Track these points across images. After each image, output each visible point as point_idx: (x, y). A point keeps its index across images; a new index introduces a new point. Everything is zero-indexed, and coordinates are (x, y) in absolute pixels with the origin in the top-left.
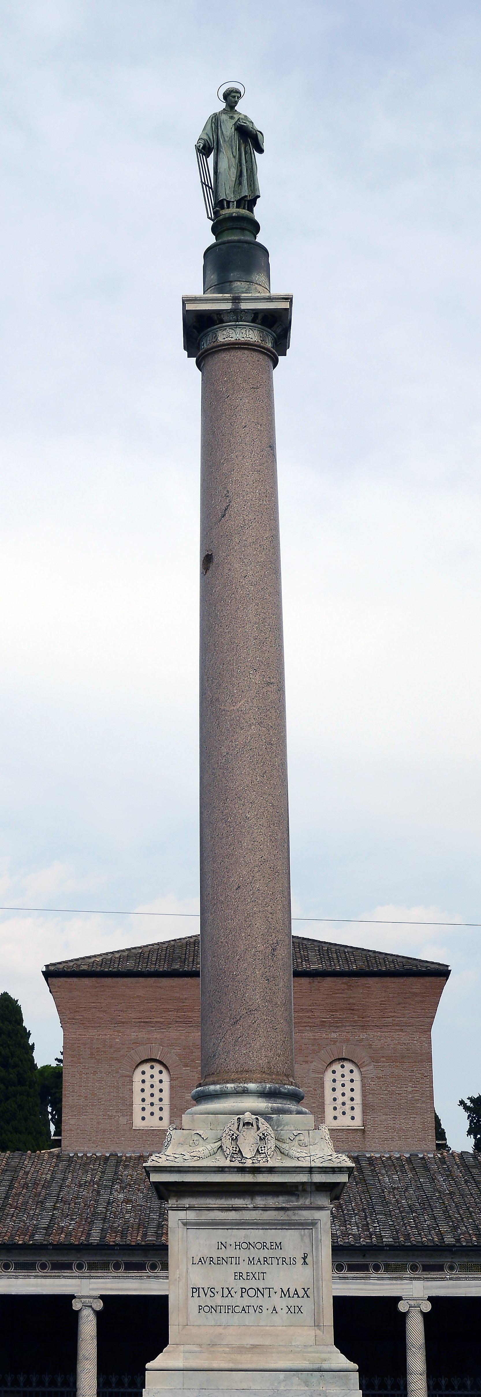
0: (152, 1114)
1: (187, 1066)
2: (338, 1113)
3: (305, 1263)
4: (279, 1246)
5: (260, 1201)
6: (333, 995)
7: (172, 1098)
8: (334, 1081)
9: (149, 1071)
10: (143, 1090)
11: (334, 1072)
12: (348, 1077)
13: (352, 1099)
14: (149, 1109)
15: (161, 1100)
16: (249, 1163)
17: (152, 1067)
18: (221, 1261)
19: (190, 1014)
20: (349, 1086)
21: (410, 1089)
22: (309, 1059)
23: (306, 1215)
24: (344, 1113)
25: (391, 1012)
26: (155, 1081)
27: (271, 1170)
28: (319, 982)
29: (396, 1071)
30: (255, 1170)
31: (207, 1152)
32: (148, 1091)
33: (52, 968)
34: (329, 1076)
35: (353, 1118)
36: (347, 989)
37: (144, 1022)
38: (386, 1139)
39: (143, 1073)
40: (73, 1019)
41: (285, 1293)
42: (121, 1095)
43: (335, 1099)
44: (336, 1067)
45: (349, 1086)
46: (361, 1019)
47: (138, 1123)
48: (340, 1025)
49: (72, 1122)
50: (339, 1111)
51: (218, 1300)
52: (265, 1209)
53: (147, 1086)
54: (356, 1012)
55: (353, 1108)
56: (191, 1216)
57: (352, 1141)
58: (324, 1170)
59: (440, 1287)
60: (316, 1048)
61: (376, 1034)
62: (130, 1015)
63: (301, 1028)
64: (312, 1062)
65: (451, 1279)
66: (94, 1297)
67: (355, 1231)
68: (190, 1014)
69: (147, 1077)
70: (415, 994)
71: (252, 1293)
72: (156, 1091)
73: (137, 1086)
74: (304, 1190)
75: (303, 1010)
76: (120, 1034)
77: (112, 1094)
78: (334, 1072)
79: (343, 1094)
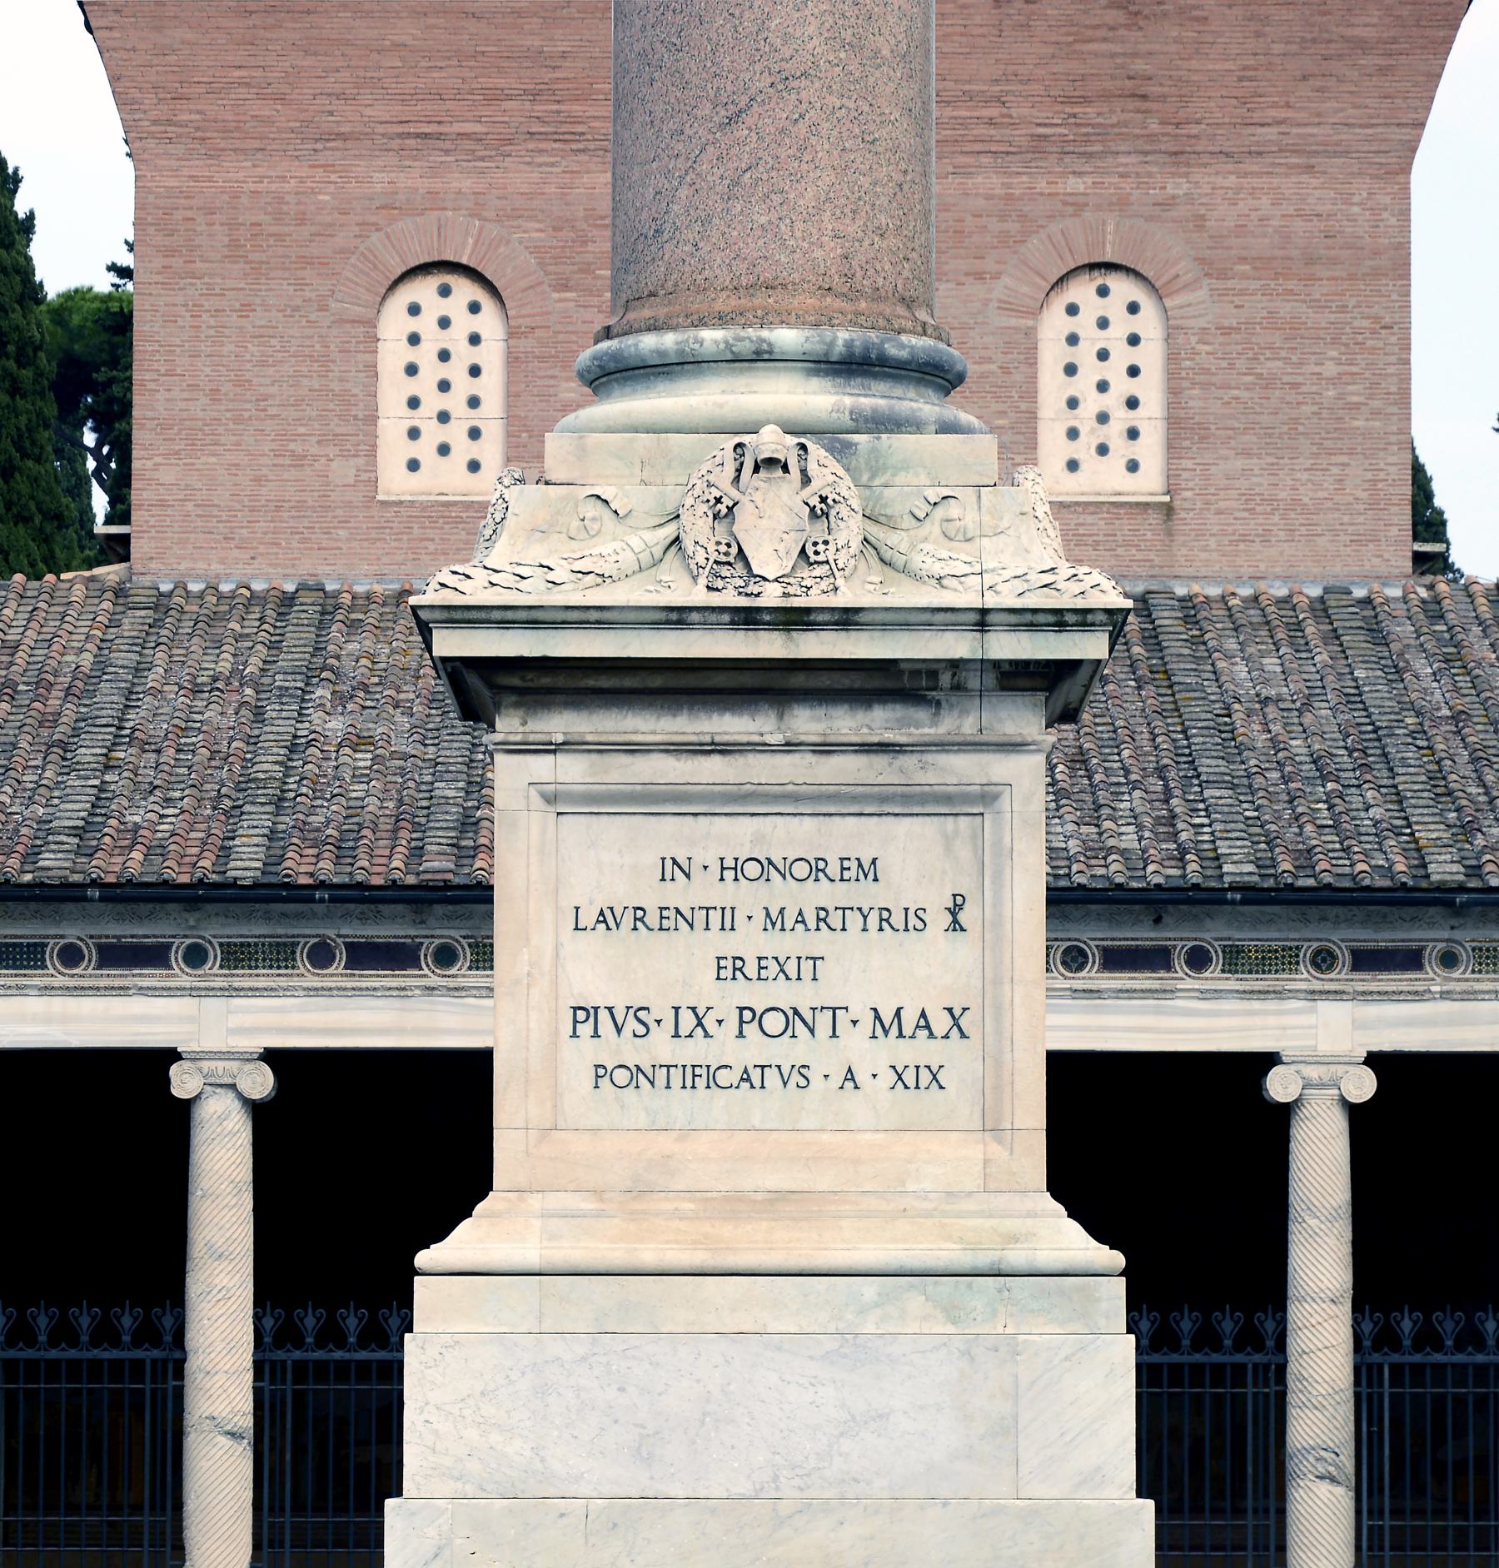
0: (444, 450)
1: (566, 287)
2: (1083, 449)
3: (956, 926)
4: (869, 870)
5: (807, 722)
6: (1078, 47)
7: (512, 396)
8: (1073, 340)
9: (434, 306)
10: (412, 370)
12: (1122, 325)
13: (1132, 403)
14: (433, 433)
15: (474, 402)
16: (771, 596)
17: (445, 291)
18: (672, 919)
19: (576, 108)
20: (1122, 356)
21: (1330, 369)
22: (989, 265)
23: (962, 769)
24: (1103, 450)
25: (1274, 105)
27: (847, 619)
29: (1285, 309)
30: (794, 619)
31: (628, 560)
34: (1053, 324)
35: (1133, 466)
36: (1128, 27)
37: (418, 136)
38: (1244, 538)
39: (414, 310)
40: (170, 123)
41: (885, 1025)
42: (336, 386)
43: (1073, 403)
44: (1082, 291)
46: (1170, 129)
47: (395, 482)
48: (1097, 148)
49: (167, 475)
51: (661, 1047)
52: (824, 748)
53: (426, 356)
54: (1154, 106)
55: (1133, 434)
56: (572, 770)
57: (1127, 544)
58: (1028, 620)
60: (1013, 227)
61: (1219, 181)
62: (368, 111)
63: (962, 160)
64: (997, 276)
67: (1129, 840)
68: (576, 108)
69: (426, 325)
70: (1361, 45)
71: (774, 1022)
72: (455, 370)
73: (392, 354)
74: (958, 687)
75: (970, 96)
76: (333, 177)
77: (305, 381)
78: (1072, 310)
79: (1103, 387)
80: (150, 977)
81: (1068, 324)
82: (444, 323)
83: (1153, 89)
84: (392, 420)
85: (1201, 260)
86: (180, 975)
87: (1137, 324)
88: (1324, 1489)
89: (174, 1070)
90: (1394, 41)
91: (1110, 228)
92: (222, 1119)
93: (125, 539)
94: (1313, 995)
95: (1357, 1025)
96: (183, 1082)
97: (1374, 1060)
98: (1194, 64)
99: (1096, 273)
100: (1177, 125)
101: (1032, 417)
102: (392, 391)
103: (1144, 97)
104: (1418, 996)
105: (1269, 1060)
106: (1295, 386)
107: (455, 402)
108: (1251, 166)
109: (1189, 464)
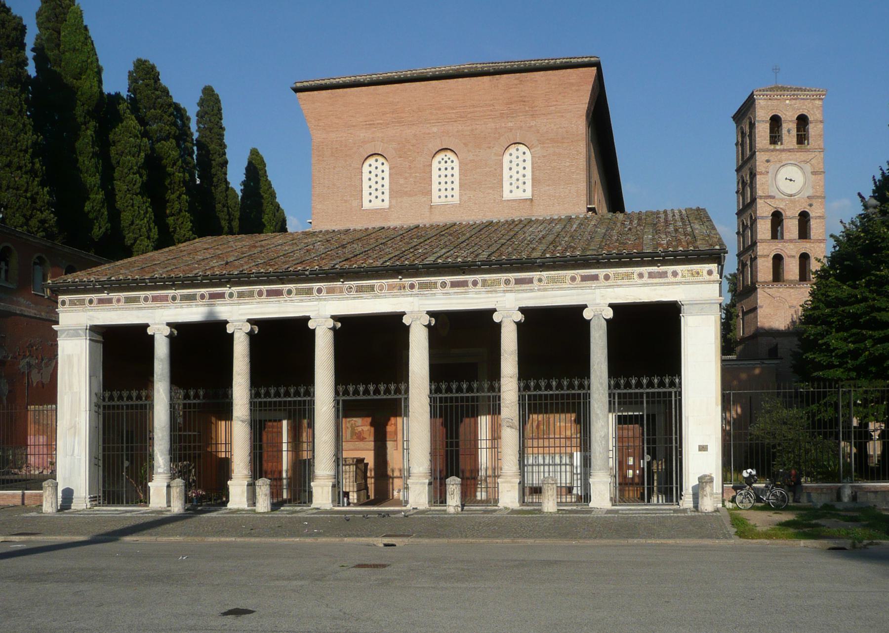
0: (377, 197)
1: (401, 157)
8: (511, 162)
9: (374, 164)
11: (511, 155)
13: (524, 176)
21: (568, 164)
24: (518, 187)
26: (379, 171)
28: (497, 80)
32: (374, 179)
34: (506, 158)
35: (524, 191)
36: (520, 84)
40: (318, 126)
42: (353, 184)
43: (511, 177)
44: (512, 149)
45: (522, 165)
47: (366, 205)
48: (515, 115)
50: (514, 185)
53: (373, 176)
54: (527, 103)
59: (530, 298)
60: (497, 135)
65: (539, 290)
69: (373, 169)
73: (366, 176)
77: (347, 183)
78: (511, 155)
84: (366, 191)
85: (538, 140)
87: (525, 157)
91: (518, 134)
95: (517, 300)
99: (516, 145)
100: (532, 108)
102: (366, 184)
103: (524, 101)
104: (532, 290)
105: (494, 310)
106: (559, 169)
107: (379, 186)
108: (550, 117)
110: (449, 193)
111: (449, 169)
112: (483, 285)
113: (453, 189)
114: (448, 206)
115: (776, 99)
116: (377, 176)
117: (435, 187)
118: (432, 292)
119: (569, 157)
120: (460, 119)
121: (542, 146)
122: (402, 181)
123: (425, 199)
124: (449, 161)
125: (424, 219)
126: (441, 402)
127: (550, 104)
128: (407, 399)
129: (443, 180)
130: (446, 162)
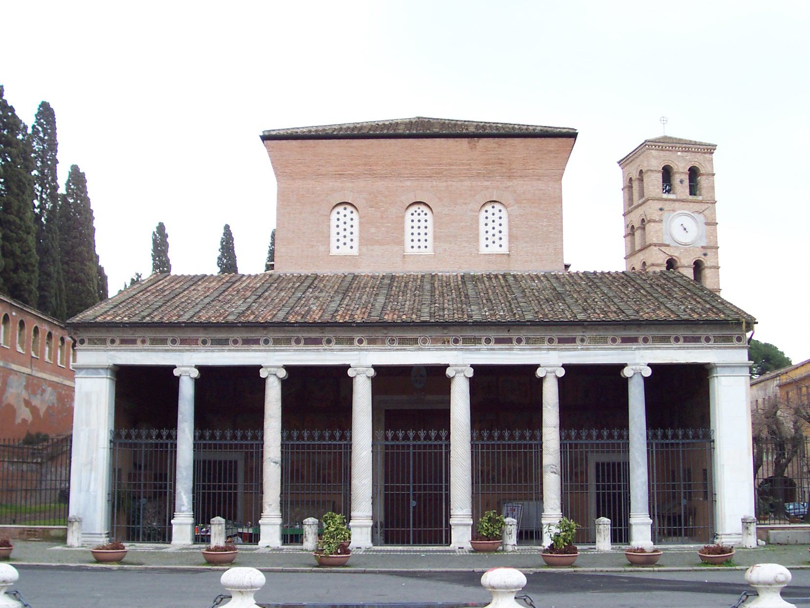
0: (345, 244)
7: (360, 231)
8: (487, 218)
12: (498, 215)
13: (500, 232)
14: (342, 240)
17: (345, 209)
19: (374, 168)
20: (498, 221)
21: (545, 224)
25: (531, 165)
26: (348, 219)
32: (342, 226)
33: (266, 134)
37: (339, 174)
38: (526, 261)
39: (338, 213)
44: (489, 207)
47: (334, 251)
48: (491, 175)
50: (491, 239)
53: (341, 223)
54: (504, 165)
55: (501, 239)
64: (469, 203)
66: (278, 367)
69: (341, 216)
70: (550, 151)
72: (348, 226)
73: (334, 222)
75: (463, 164)
78: (486, 211)
80: (255, 347)
81: (485, 214)
82: (345, 216)
83: (504, 162)
84: (334, 237)
85: (516, 200)
86: (262, 347)
88: (553, 475)
89: (261, 370)
90: (558, 150)
91: (495, 193)
92: (273, 383)
93: (273, 265)
94: (548, 349)
95: (560, 357)
96: (263, 374)
97: (564, 366)
98: (513, 156)
101: (478, 235)
102: (334, 231)
103: (502, 163)
104: (575, 349)
106: (537, 227)
107: (347, 233)
108: (526, 179)
109: (513, 245)
110: (423, 244)
111: (423, 221)
112: (527, 343)
113: (426, 240)
114: (422, 257)
115: (668, 150)
116: (345, 223)
117: (408, 237)
118: (476, 347)
119: (546, 217)
120: (435, 175)
121: (518, 205)
122: (373, 230)
123: (397, 249)
124: (422, 214)
125: (399, 269)
126: (482, 448)
127: (527, 168)
128: (448, 446)
129: (416, 231)
130: (419, 214)
